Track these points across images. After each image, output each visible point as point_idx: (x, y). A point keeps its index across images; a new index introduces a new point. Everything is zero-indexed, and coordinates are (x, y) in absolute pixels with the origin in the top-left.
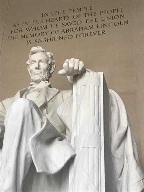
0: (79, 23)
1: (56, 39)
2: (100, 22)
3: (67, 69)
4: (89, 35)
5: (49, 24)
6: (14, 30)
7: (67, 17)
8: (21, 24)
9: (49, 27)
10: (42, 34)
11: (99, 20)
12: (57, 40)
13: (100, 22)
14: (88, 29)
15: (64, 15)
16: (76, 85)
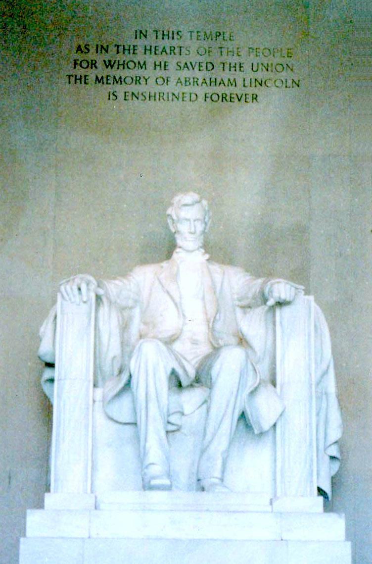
0: (210, 67)
1: (165, 97)
2: (249, 75)
3: (277, 301)
4: (228, 98)
5: (150, 59)
6: (79, 62)
7: (186, 49)
8: (93, 50)
9: (150, 66)
10: (137, 80)
11: (247, 67)
12: (168, 100)
13: (249, 75)
14: (226, 84)
15: (181, 44)
16: (280, 309)
